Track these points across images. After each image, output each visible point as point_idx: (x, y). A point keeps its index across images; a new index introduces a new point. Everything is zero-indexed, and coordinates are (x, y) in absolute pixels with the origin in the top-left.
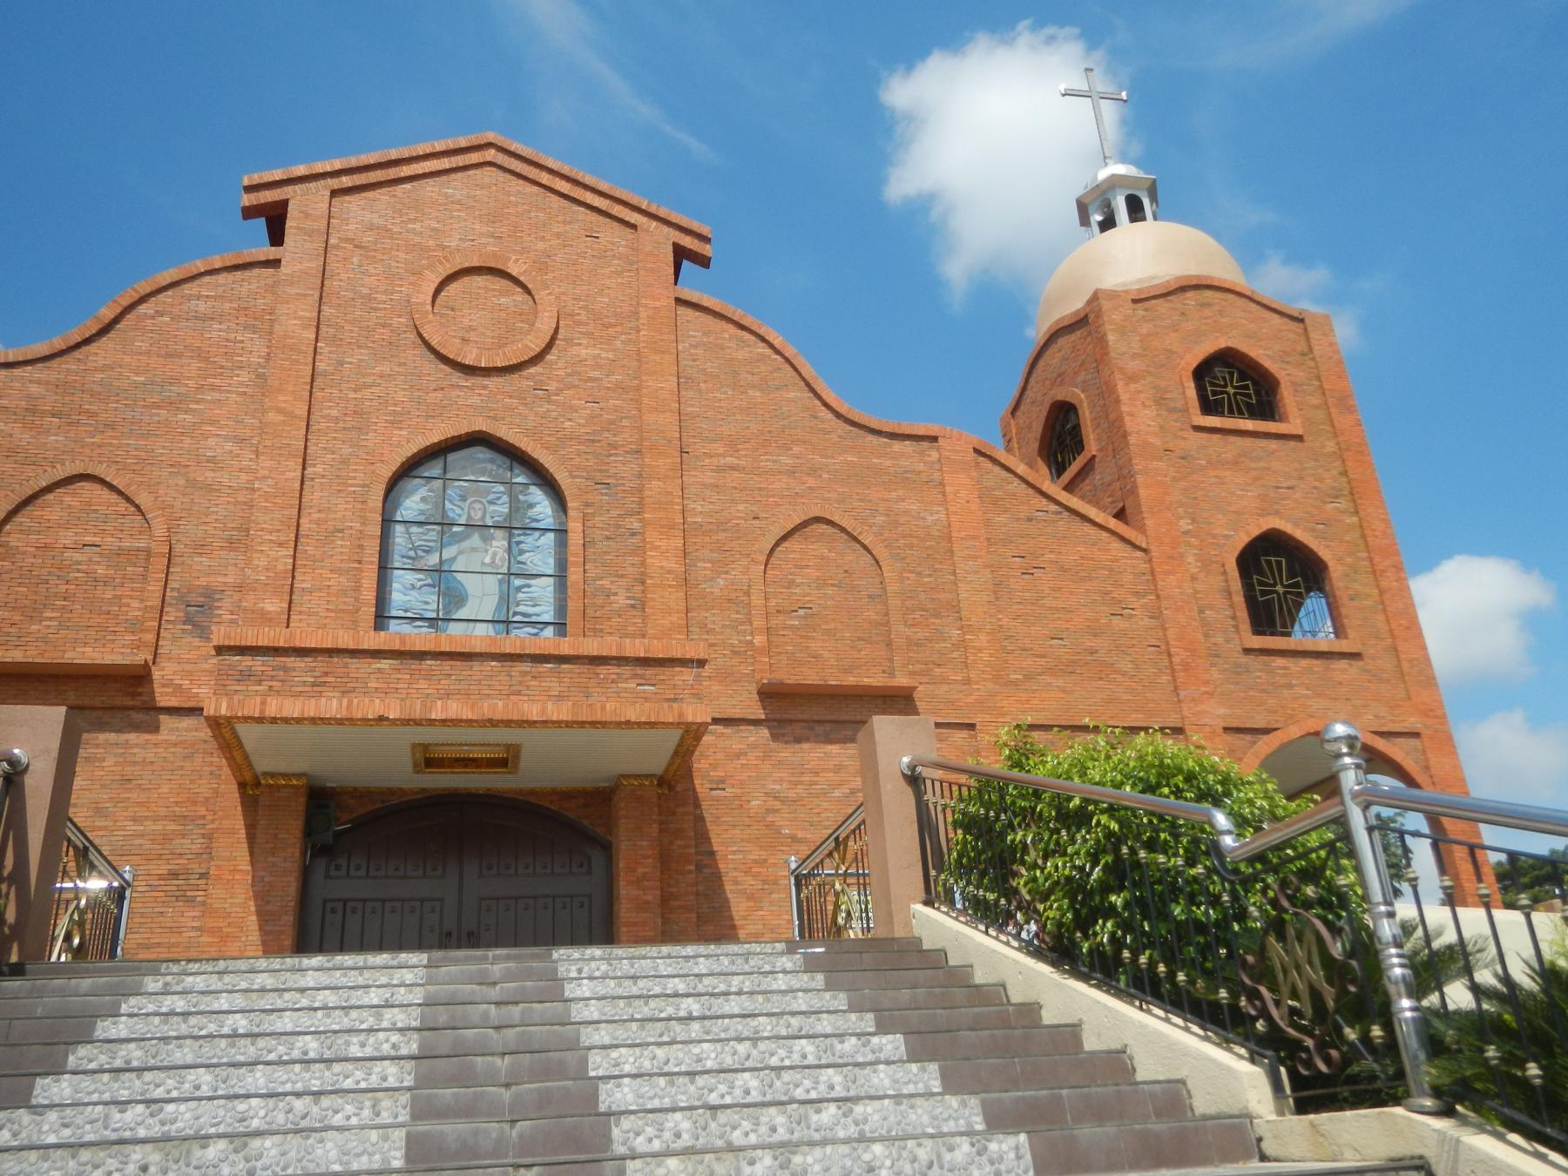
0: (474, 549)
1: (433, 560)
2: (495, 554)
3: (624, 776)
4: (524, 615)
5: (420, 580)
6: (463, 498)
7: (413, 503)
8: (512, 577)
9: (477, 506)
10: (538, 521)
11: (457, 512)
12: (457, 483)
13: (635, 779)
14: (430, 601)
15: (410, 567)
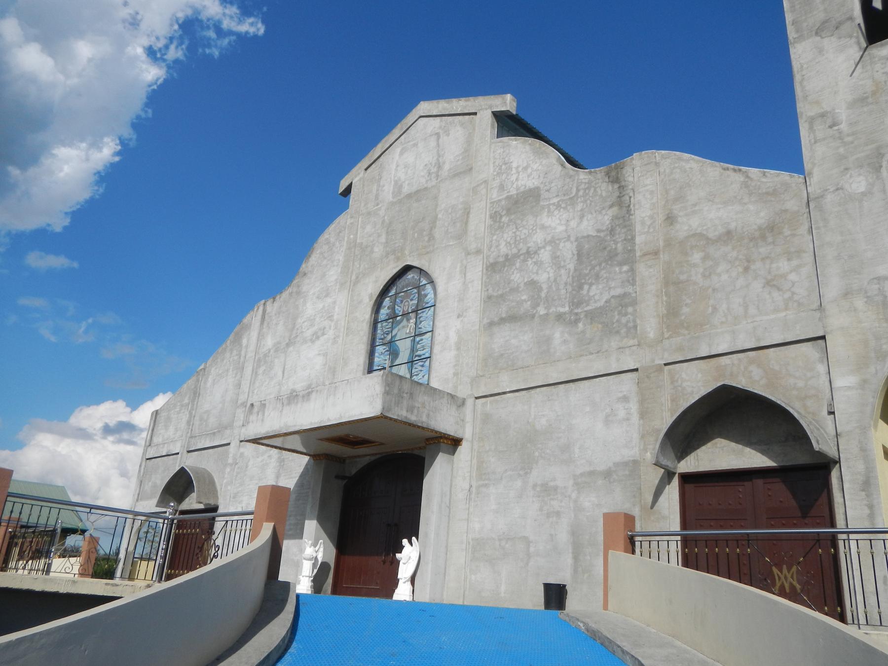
0: (404, 327)
1: (389, 337)
2: (411, 327)
3: (428, 440)
4: (419, 356)
5: (384, 349)
6: (402, 301)
7: (384, 312)
8: (416, 337)
9: (407, 304)
10: (428, 303)
11: (399, 310)
12: (400, 295)
13: (432, 440)
14: (387, 358)
15: (381, 343)
